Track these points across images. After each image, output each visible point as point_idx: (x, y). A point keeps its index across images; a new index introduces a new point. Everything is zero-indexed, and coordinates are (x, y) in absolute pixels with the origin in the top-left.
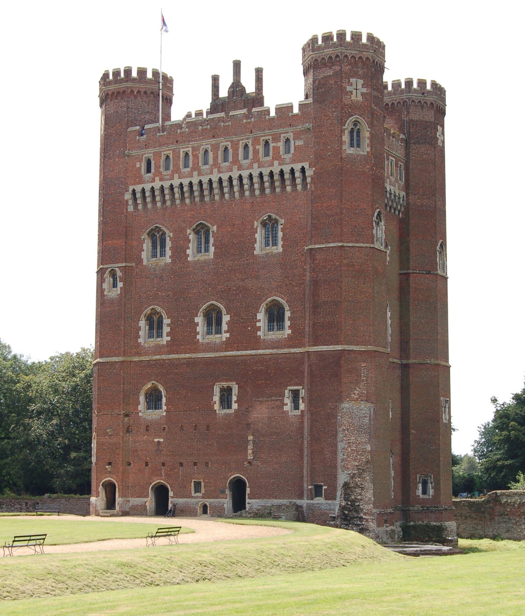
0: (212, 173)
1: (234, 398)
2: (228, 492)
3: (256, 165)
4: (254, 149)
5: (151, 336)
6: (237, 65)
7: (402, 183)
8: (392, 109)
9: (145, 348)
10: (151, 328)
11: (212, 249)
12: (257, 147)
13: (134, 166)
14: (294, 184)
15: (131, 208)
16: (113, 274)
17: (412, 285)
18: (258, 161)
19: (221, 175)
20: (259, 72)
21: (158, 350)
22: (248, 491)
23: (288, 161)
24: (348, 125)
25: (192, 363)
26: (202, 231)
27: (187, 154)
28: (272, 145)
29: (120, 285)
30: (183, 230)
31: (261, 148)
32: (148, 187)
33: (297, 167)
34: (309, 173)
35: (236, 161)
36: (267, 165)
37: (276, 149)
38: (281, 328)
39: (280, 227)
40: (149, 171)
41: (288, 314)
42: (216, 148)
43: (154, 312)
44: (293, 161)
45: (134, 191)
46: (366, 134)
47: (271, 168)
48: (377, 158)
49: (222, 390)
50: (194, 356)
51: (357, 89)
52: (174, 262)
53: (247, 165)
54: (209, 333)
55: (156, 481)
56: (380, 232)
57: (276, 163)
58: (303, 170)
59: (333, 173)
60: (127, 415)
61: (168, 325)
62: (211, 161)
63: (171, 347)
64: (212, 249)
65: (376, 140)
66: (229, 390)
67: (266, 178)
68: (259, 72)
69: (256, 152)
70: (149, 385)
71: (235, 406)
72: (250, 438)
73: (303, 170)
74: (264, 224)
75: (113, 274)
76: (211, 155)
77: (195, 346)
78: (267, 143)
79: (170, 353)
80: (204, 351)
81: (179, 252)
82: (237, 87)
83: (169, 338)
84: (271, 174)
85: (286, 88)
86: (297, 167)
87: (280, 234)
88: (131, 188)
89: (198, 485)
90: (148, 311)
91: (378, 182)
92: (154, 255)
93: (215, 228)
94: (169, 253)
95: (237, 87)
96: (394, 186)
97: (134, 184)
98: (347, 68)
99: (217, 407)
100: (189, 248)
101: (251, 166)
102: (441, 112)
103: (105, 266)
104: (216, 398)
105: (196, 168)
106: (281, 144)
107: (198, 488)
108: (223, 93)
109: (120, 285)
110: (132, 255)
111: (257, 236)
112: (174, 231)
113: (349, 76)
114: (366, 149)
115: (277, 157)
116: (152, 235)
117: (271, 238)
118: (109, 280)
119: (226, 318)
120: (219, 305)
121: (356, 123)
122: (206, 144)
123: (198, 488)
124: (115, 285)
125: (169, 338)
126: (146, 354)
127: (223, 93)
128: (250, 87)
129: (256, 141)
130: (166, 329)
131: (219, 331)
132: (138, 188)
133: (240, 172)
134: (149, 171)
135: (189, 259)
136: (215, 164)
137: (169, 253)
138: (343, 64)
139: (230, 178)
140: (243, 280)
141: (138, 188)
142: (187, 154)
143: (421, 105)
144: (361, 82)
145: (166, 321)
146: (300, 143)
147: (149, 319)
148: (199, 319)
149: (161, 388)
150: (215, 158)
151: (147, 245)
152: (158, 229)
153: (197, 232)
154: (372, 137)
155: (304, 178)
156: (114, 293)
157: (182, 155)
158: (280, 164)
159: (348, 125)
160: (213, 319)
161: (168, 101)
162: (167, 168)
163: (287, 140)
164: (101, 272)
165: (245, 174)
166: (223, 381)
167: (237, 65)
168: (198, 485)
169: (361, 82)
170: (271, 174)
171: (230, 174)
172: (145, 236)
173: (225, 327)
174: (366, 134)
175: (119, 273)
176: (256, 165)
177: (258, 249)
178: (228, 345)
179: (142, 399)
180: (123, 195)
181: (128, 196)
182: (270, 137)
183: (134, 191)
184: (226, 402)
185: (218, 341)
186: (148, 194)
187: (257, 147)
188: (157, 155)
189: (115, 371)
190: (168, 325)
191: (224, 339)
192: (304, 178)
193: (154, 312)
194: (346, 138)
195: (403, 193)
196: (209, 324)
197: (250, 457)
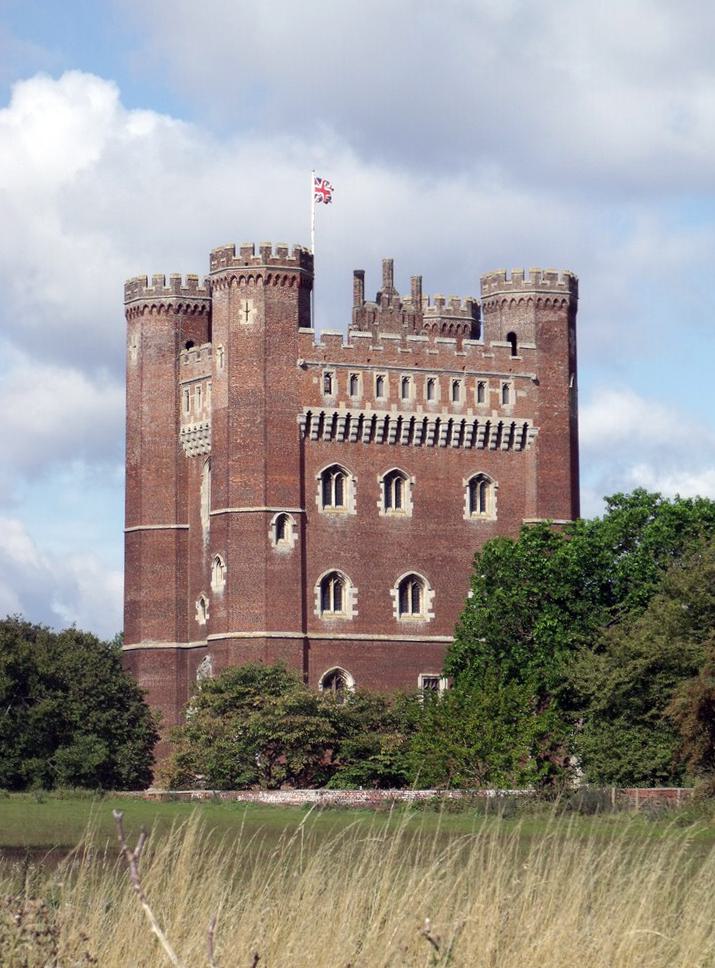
0: (415, 410)
3: (470, 411)
4: (468, 391)
6: (389, 268)
9: (323, 623)
12: (472, 389)
13: (309, 381)
18: (473, 406)
19: (426, 415)
20: (418, 284)
21: (343, 625)
23: (508, 412)
30: (371, 475)
31: (475, 390)
32: (329, 413)
33: (520, 423)
36: (484, 413)
44: (516, 413)
45: (309, 414)
47: (489, 418)
50: (392, 638)
52: (360, 515)
53: (460, 409)
57: (495, 412)
61: (355, 596)
63: (359, 624)
68: (418, 284)
73: (526, 425)
78: (481, 386)
79: (358, 632)
80: (402, 633)
82: (386, 297)
83: (356, 613)
86: (520, 423)
88: (306, 410)
93: (413, 478)
95: (386, 297)
97: (310, 405)
100: (380, 500)
101: (463, 411)
103: (273, 509)
106: (500, 391)
108: (370, 297)
109: (291, 537)
112: (361, 475)
120: (422, 576)
124: (280, 534)
125: (356, 613)
126: (324, 630)
127: (370, 297)
128: (405, 295)
132: (316, 412)
133: (451, 416)
135: (381, 513)
140: (450, 550)
141: (316, 412)
142: (380, 380)
146: (522, 394)
148: (395, 592)
158: (499, 416)
166: (429, 671)
167: (389, 268)
171: (438, 415)
176: (470, 411)
177: (466, 516)
180: (294, 416)
181: (301, 419)
182: (487, 380)
183: (309, 414)
185: (420, 622)
187: (472, 389)
189: (291, 650)
190: (355, 596)
191: (429, 620)
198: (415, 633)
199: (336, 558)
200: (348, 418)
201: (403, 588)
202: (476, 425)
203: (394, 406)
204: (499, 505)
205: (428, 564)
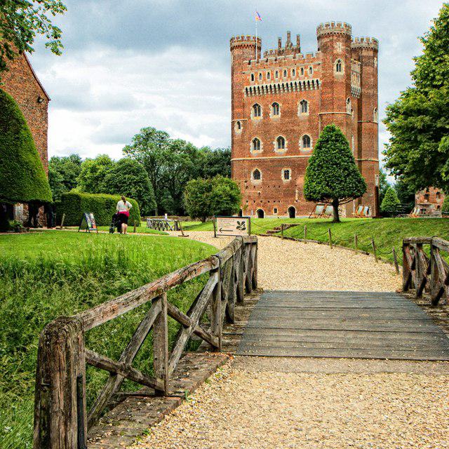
1: (290, 175)
2: (288, 213)
5: (255, 149)
6: (289, 34)
7: (359, 83)
8: (354, 50)
10: (255, 146)
11: (280, 114)
14: (314, 87)
15: (245, 96)
16: (239, 123)
17: (363, 127)
21: (259, 155)
22: (296, 212)
24: (336, 62)
25: (272, 161)
26: (275, 105)
27: (269, 73)
28: (304, 70)
29: (242, 128)
30: (267, 105)
31: (300, 71)
33: (315, 80)
34: (320, 82)
35: (289, 77)
37: (306, 72)
38: (309, 146)
39: (308, 105)
40: (253, 80)
41: (311, 141)
42: (281, 71)
43: (256, 139)
45: (247, 89)
46: (343, 66)
48: (348, 77)
49: (285, 171)
51: (339, 47)
52: (264, 118)
54: (279, 148)
55: (259, 208)
56: (349, 106)
58: (317, 81)
59: (330, 84)
60: (246, 182)
62: (279, 77)
63: (265, 153)
64: (280, 114)
65: (348, 68)
66: (288, 171)
67: (302, 84)
69: (298, 73)
70: (255, 169)
71: (290, 178)
72: (297, 191)
73: (317, 81)
74: (301, 103)
75: (239, 123)
76: (279, 74)
77: (274, 154)
79: (263, 156)
81: (266, 114)
82: (289, 44)
84: (304, 83)
85: (310, 47)
86: (315, 80)
87: (308, 108)
89: (276, 210)
90: (253, 139)
91: (348, 87)
92: (256, 116)
94: (262, 115)
95: (289, 44)
96: (355, 84)
98: (335, 38)
99: (283, 178)
102: (376, 51)
104: (283, 175)
105: (273, 79)
106: (308, 70)
107: (276, 212)
110: (244, 115)
111: (299, 108)
113: (336, 41)
114: (343, 73)
115: (306, 75)
116: (254, 106)
117: (304, 110)
118: (236, 125)
119: (286, 142)
121: (339, 61)
122: (278, 69)
123: (276, 212)
124: (239, 128)
127: (283, 45)
128: (295, 44)
129: (298, 68)
130: (261, 147)
131: (283, 148)
132: (248, 88)
134: (253, 80)
136: (281, 78)
137: (262, 115)
138: (333, 38)
139: (287, 84)
141: (248, 88)
143: (367, 49)
144: (341, 44)
145: (261, 143)
147: (254, 142)
148: (275, 143)
149: (260, 171)
150: (281, 75)
151: (253, 111)
152: (257, 105)
153: (273, 105)
154: (346, 67)
155: (318, 85)
156: (238, 132)
157: (267, 74)
159: (336, 62)
160: (281, 142)
161: (260, 49)
162: (260, 79)
163: (311, 68)
164: (233, 123)
165: (293, 82)
167: (289, 34)
168: (276, 210)
169: (341, 44)
170: (304, 83)
172: (251, 108)
173: (286, 146)
174: (343, 66)
175: (241, 123)
177: (299, 114)
178: (287, 153)
179: (252, 175)
180: (241, 90)
181: (244, 91)
183: (247, 89)
184: (287, 176)
186: (253, 90)
188: (256, 73)
192: (318, 85)
193: (256, 139)
194: (335, 68)
195: (359, 88)
196: (279, 145)
197: (297, 199)
198: (281, 155)
199: (257, 134)
200: (258, 88)
201: (278, 140)
202: (300, 83)
203: (273, 81)
204: (310, 110)
205: (286, 132)
